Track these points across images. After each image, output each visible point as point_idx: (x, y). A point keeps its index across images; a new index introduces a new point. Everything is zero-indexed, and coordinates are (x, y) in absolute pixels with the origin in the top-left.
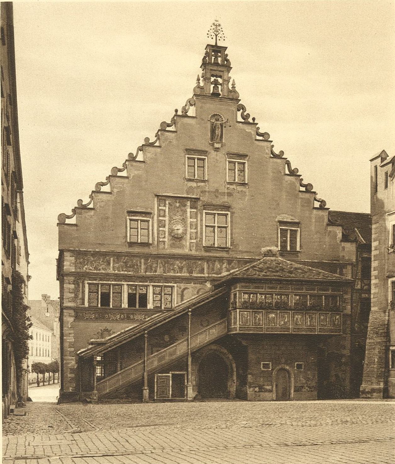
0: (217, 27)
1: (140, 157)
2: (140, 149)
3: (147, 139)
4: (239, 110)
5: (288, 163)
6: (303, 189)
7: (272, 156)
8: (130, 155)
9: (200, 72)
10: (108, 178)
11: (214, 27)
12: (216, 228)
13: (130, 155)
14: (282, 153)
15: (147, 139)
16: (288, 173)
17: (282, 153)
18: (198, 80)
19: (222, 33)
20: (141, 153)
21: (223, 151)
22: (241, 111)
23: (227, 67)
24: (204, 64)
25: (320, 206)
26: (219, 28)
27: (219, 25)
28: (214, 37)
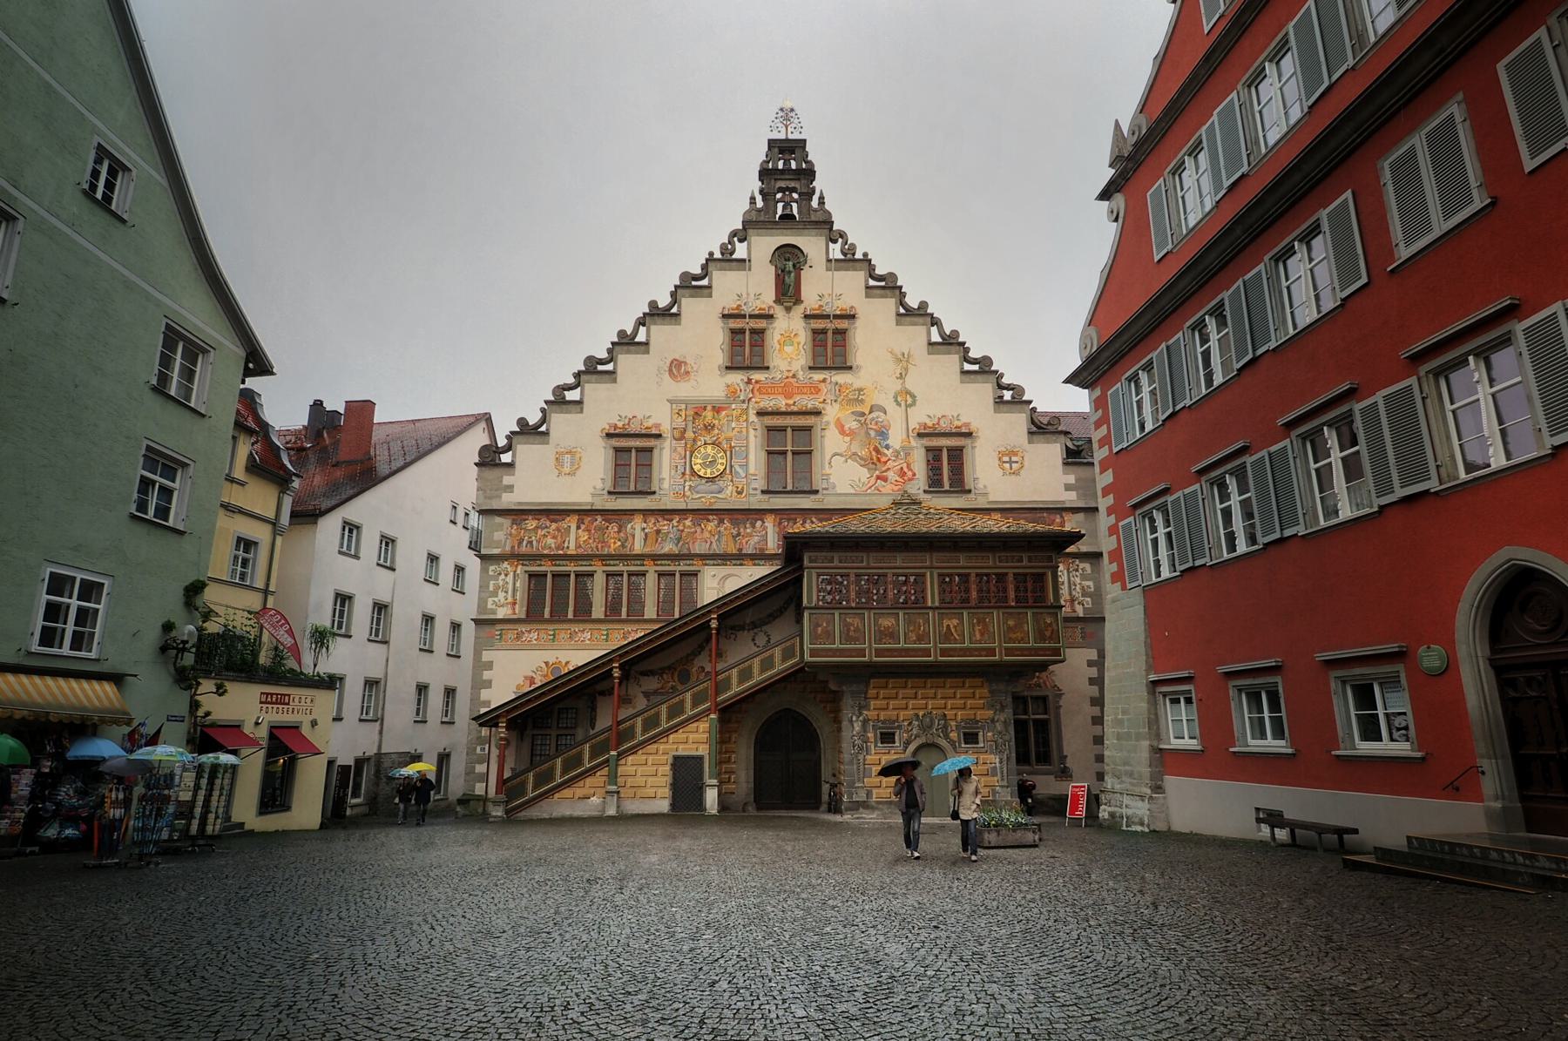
0: (787, 115)
1: (641, 337)
2: (641, 322)
3: (653, 304)
4: (835, 242)
5: (935, 322)
6: (976, 367)
7: (902, 311)
8: (622, 334)
9: (756, 185)
10: (578, 375)
11: (781, 114)
12: (790, 455)
13: (622, 334)
14: (923, 305)
15: (653, 304)
16: (940, 340)
17: (923, 305)
18: (753, 199)
19: (796, 121)
20: (642, 330)
21: (798, 311)
22: (840, 240)
23: (809, 174)
24: (764, 174)
25: (1013, 397)
26: (793, 114)
27: (792, 110)
28: (784, 130)
